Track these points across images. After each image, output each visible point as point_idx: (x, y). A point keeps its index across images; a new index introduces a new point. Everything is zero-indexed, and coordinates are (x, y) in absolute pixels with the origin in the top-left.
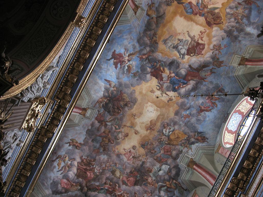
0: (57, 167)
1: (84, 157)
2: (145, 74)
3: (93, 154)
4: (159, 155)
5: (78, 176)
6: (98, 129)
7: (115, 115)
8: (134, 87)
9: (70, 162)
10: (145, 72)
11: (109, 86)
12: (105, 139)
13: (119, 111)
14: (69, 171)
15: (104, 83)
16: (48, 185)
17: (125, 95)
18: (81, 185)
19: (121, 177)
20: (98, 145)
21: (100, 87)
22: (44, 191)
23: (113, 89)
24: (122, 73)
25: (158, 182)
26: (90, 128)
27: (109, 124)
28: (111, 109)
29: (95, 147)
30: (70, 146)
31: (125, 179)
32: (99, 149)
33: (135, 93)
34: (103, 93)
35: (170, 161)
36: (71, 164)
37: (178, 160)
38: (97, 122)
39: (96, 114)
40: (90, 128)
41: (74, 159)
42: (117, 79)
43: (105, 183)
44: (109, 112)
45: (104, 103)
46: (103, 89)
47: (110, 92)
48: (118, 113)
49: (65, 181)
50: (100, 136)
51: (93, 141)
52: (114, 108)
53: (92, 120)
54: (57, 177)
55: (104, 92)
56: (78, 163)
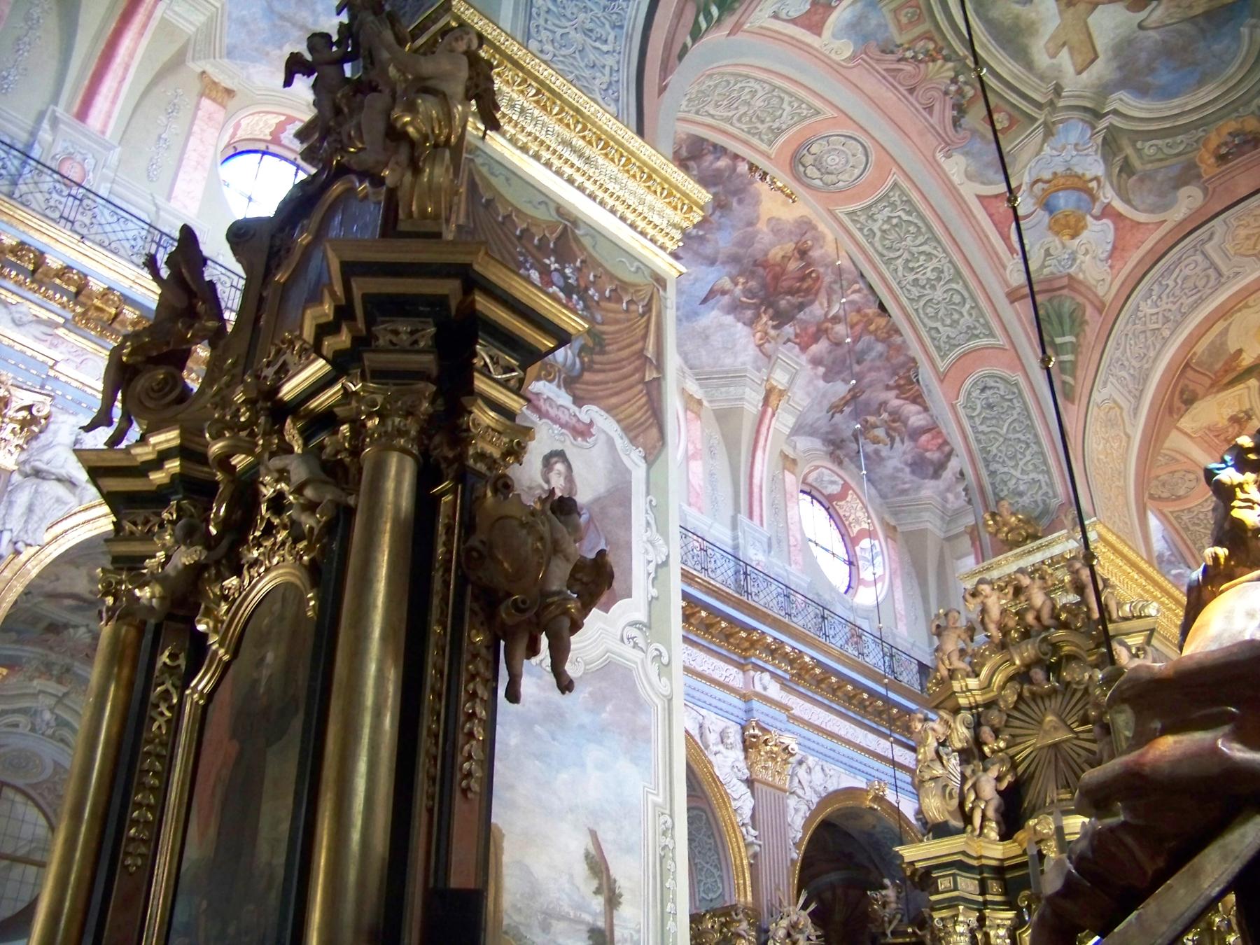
0: (880, 446)
1: (892, 383)
2: (730, 177)
3: (894, 361)
6: (838, 344)
7: (819, 288)
8: (758, 218)
9: (885, 416)
10: (727, 174)
11: (727, 297)
12: (872, 327)
13: (814, 275)
14: (905, 423)
15: (713, 309)
16: (912, 481)
17: (770, 255)
20: (880, 347)
21: (721, 326)
22: (920, 499)
23: (740, 287)
24: (702, 244)
26: (821, 370)
27: (835, 309)
28: (795, 300)
29: (881, 355)
30: (842, 411)
32: (889, 346)
33: (779, 219)
34: (740, 325)
36: (890, 414)
38: (815, 349)
39: (790, 350)
40: (821, 370)
42: (712, 262)
44: (801, 307)
45: (770, 323)
46: (730, 319)
47: (744, 299)
48: (818, 278)
49: (924, 438)
50: (856, 340)
51: (859, 362)
52: (799, 290)
53: (804, 363)
54: (904, 453)
55: (739, 320)
56: (897, 397)
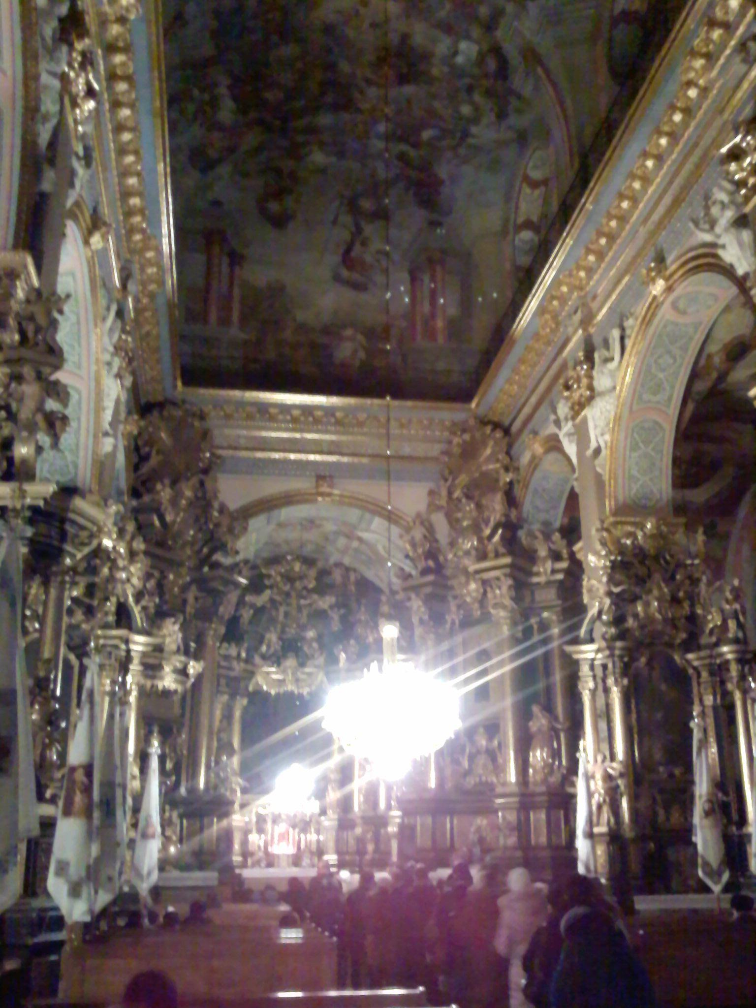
4: (442, 14)
5: (243, 110)
9: (206, 97)
18: (261, 122)
19: (359, 73)
25: (460, 77)
31: (369, 74)
35: (476, 32)
37: (499, 34)
40: (215, 24)
41: (215, 85)
43: (323, 94)
